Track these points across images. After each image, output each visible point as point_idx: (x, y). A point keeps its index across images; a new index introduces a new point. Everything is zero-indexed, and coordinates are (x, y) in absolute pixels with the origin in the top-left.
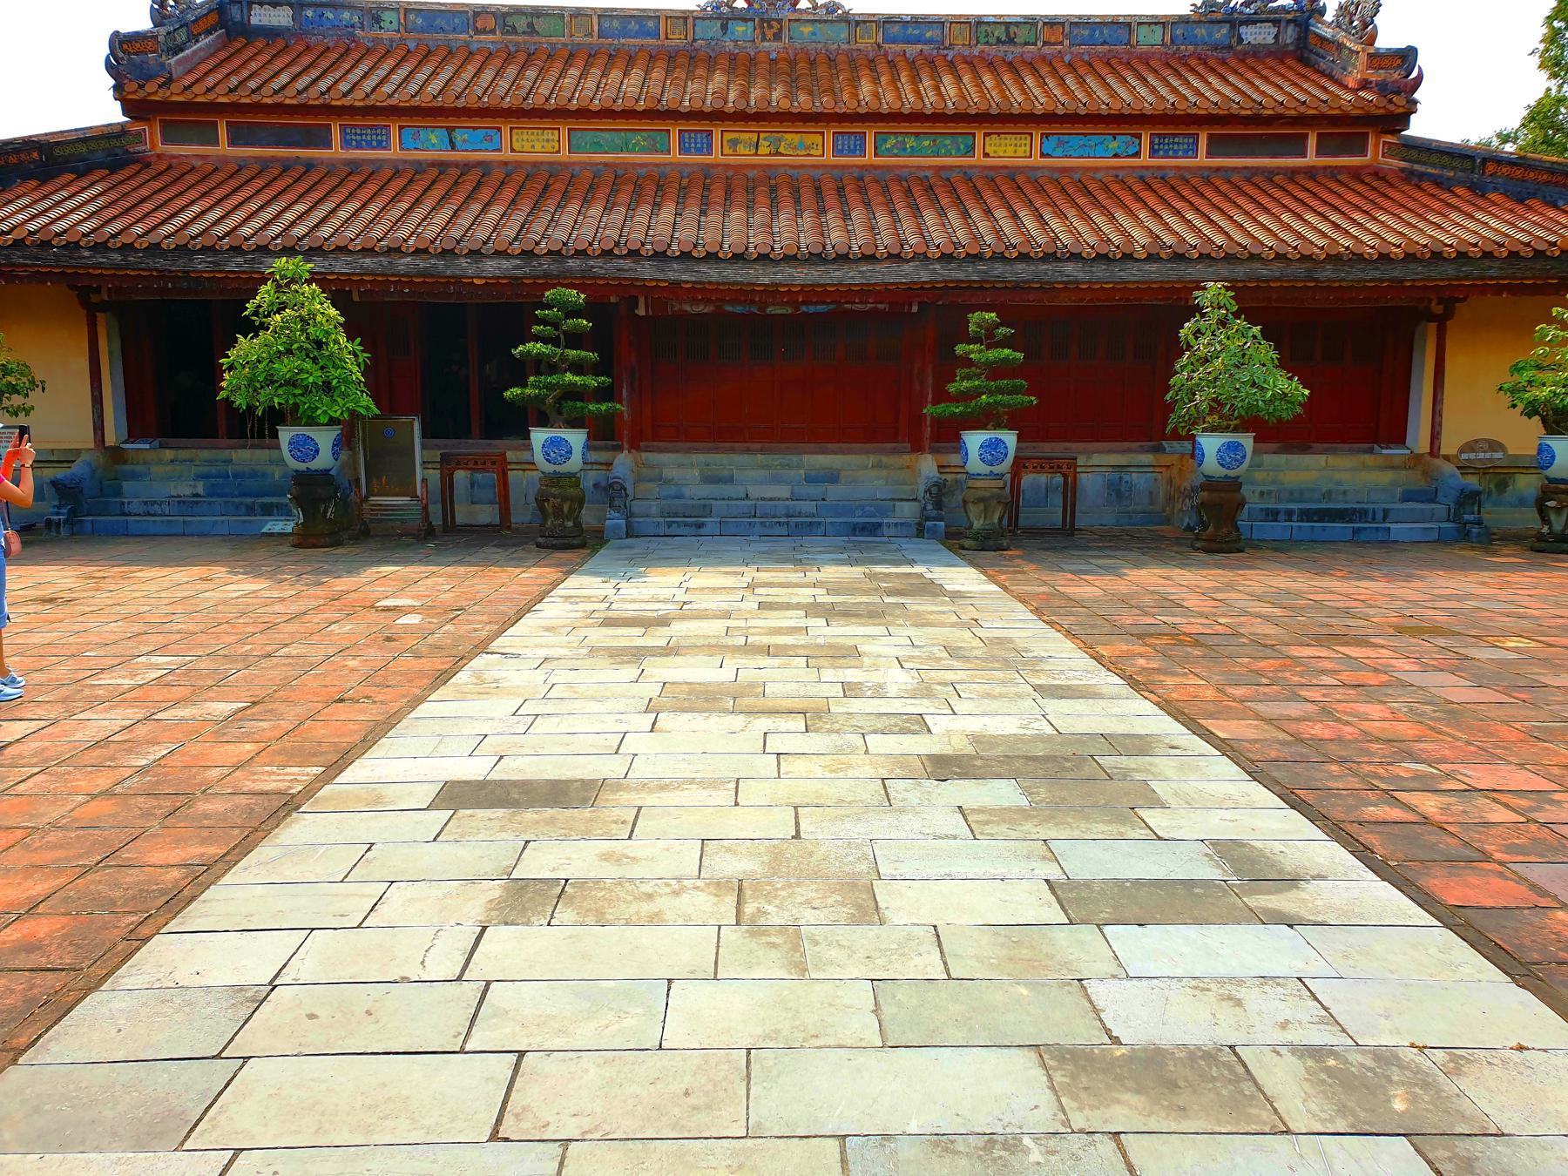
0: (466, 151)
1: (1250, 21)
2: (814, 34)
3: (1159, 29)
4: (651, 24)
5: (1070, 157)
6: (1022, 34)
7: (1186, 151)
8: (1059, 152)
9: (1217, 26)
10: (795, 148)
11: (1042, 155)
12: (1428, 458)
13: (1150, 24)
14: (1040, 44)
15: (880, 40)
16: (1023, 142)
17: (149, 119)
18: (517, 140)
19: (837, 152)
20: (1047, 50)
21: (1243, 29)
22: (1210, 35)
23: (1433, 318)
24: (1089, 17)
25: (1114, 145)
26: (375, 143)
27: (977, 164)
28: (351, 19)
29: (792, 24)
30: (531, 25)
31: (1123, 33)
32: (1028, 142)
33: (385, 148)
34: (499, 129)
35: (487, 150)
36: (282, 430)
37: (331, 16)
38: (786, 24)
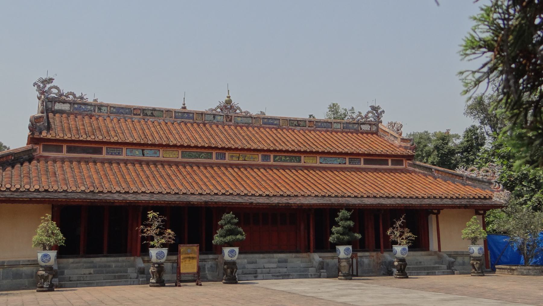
0: (148, 157)
1: (363, 124)
2: (241, 121)
3: (339, 124)
4: (191, 115)
6: (302, 123)
7: (358, 163)
8: (324, 162)
9: (355, 125)
10: (250, 159)
12: (438, 252)
13: (337, 123)
14: (307, 127)
15: (261, 123)
16: (314, 159)
17: (39, 144)
18: (165, 154)
19: (263, 160)
21: (362, 126)
22: (353, 127)
23: (434, 214)
24: (321, 120)
25: (339, 160)
26: (117, 153)
27: (303, 165)
28: (91, 108)
29: (235, 117)
31: (329, 124)
32: (316, 159)
33: (120, 155)
34: (159, 150)
35: (155, 157)
36: (151, 250)
37: (83, 107)
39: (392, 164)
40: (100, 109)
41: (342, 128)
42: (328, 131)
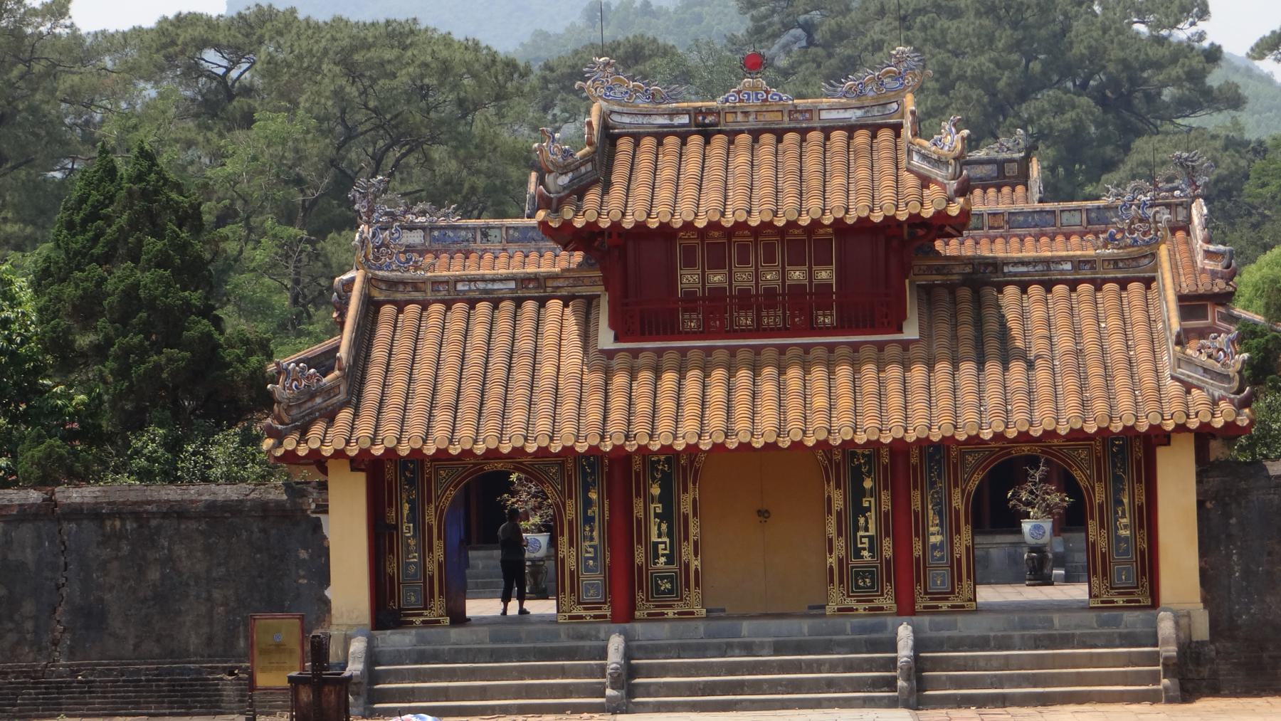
3: (1077, 214)
13: (1070, 211)
40: (485, 235)
41: (1085, 223)
42: (1044, 235)
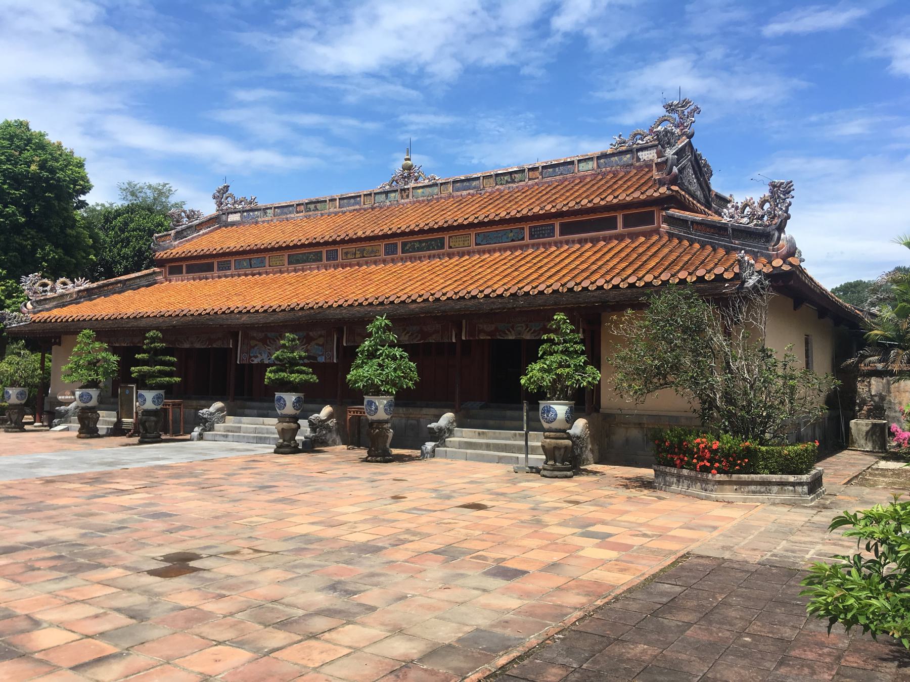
5: (490, 244)
11: (477, 244)
20: (530, 182)
21: (640, 154)
22: (620, 160)
30: (315, 207)
38: (411, 190)
39: (625, 226)
